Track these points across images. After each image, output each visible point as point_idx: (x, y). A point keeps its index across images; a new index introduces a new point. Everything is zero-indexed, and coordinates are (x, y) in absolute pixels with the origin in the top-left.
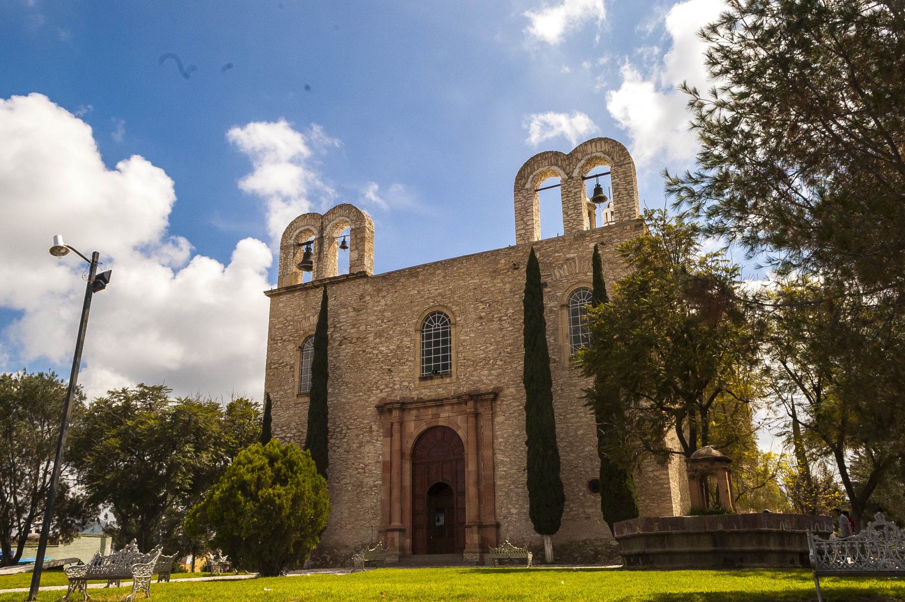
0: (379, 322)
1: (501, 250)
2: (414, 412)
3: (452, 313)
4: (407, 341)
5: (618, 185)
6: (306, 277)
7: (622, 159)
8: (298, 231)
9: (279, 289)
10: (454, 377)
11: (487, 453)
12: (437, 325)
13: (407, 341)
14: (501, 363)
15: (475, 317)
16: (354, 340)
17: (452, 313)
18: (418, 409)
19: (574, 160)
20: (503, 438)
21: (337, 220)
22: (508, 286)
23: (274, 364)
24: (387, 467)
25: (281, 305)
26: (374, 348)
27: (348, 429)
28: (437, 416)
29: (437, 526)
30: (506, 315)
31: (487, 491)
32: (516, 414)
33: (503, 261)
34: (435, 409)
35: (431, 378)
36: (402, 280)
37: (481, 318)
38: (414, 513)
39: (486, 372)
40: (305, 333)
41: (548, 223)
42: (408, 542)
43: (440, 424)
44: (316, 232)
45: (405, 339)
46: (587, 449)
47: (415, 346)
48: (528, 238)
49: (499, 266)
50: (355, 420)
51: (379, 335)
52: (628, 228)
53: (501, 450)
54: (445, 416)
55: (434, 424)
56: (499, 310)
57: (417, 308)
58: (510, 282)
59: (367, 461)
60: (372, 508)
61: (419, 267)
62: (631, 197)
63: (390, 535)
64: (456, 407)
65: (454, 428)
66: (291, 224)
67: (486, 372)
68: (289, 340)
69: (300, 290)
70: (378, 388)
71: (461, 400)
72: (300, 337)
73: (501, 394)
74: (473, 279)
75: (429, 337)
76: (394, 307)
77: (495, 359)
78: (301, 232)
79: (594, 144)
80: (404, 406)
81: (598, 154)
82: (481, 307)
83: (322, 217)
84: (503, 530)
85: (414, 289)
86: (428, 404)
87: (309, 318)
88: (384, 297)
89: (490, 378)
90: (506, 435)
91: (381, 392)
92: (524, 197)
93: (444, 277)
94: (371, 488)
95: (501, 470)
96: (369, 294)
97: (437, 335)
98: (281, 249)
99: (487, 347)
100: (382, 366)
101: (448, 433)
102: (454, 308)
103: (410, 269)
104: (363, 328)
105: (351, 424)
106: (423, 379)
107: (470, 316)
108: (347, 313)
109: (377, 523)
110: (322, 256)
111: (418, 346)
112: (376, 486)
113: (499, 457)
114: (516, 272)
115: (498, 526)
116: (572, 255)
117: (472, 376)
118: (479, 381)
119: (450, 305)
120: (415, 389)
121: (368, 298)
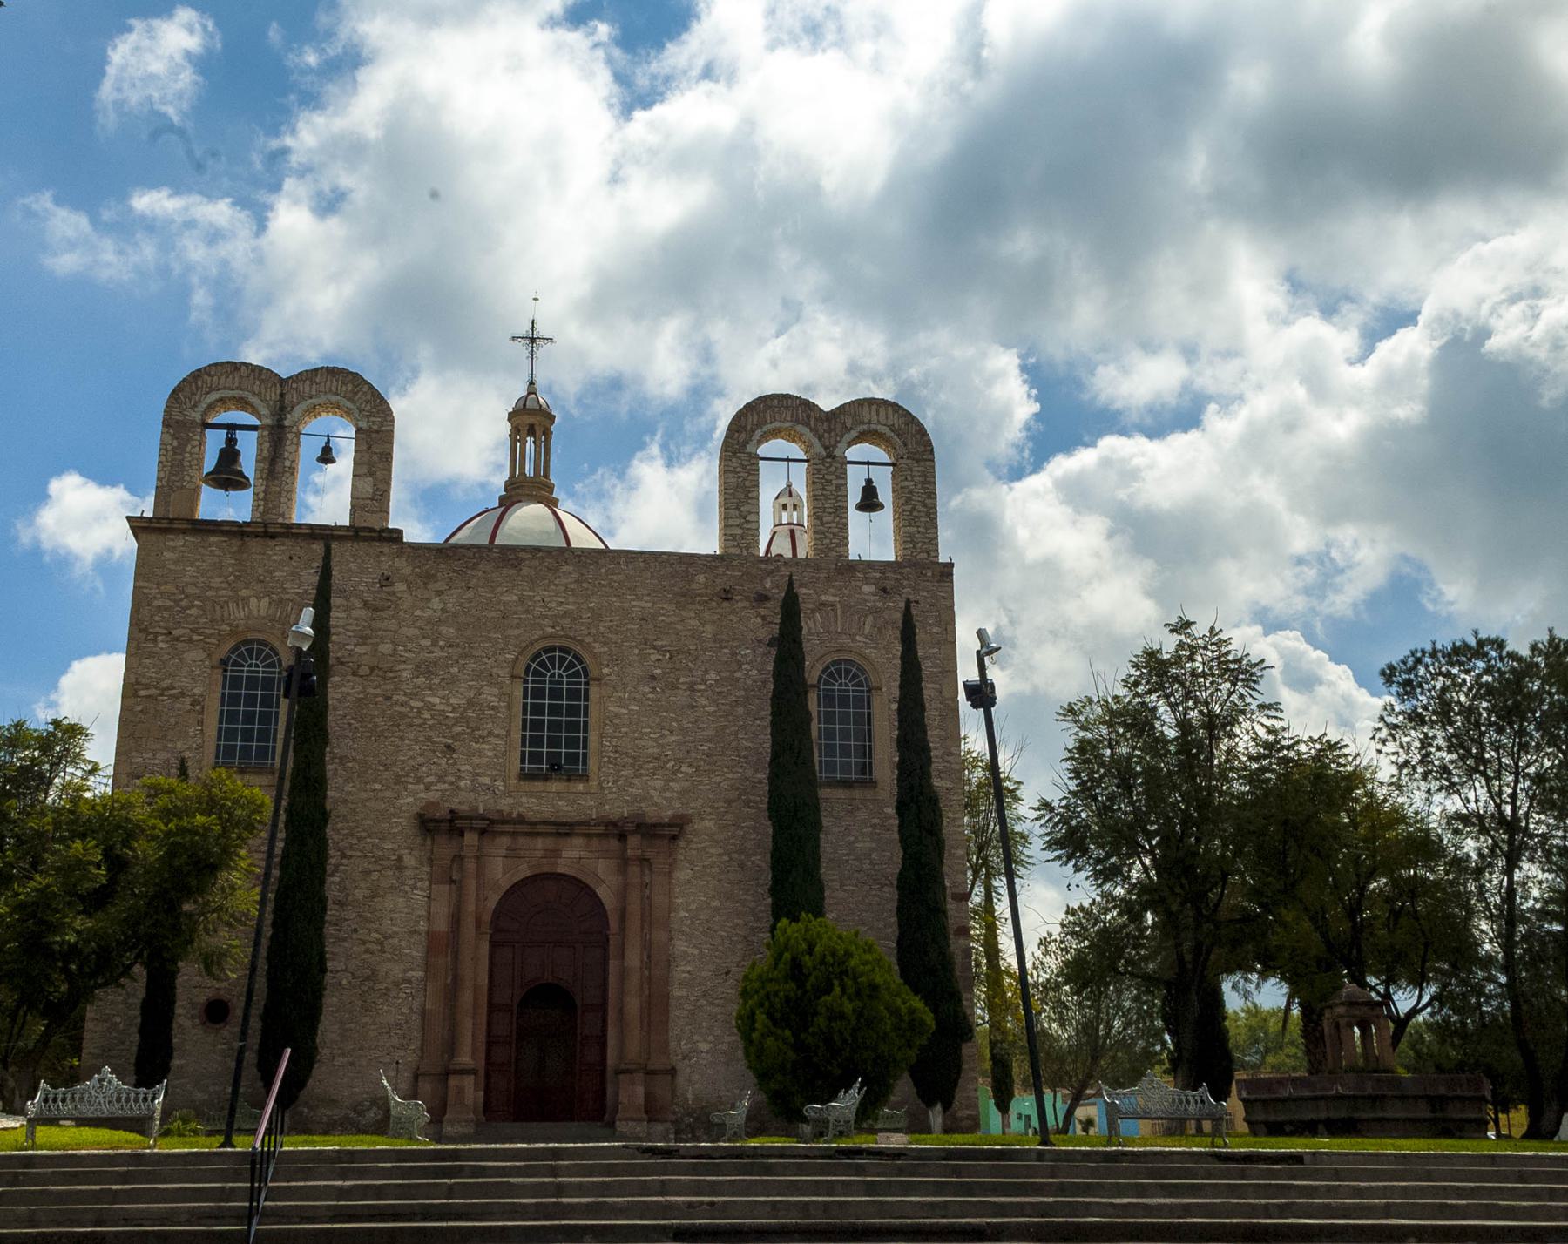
4: (490, 695)
5: (911, 492)
6: (235, 507)
8: (214, 396)
9: (155, 519)
11: (659, 936)
12: (556, 676)
13: (490, 695)
14: (690, 771)
15: (639, 672)
16: (365, 670)
17: (595, 656)
18: (514, 834)
19: (839, 427)
21: (322, 398)
22: (708, 627)
23: (147, 687)
24: (443, 945)
25: (168, 555)
26: (413, 696)
27: (343, 856)
28: (555, 853)
30: (704, 682)
31: (657, 1005)
34: (549, 842)
37: (653, 678)
39: (659, 784)
40: (233, 633)
41: (775, 525)
43: (560, 870)
44: (264, 411)
47: (509, 707)
48: (748, 547)
49: (694, 586)
50: (359, 839)
54: (572, 857)
57: (516, 632)
60: (399, 1026)
64: (595, 842)
66: (196, 376)
68: (190, 641)
70: (419, 780)
71: (617, 830)
73: (688, 828)
74: (638, 598)
75: (537, 693)
76: (463, 619)
78: (222, 400)
79: (874, 407)
80: (489, 826)
81: (883, 429)
82: (653, 658)
83: (282, 382)
85: (509, 591)
86: (541, 828)
87: (246, 600)
88: (439, 593)
89: (668, 795)
90: (693, 907)
91: (427, 789)
92: (742, 466)
94: (397, 984)
95: (681, 971)
96: (404, 580)
97: (556, 694)
98: (166, 423)
99: (663, 736)
101: (581, 889)
102: (598, 648)
105: (351, 847)
106: (525, 776)
108: (348, 609)
109: (410, 1057)
110: (279, 467)
113: (680, 945)
114: (726, 604)
116: (831, 599)
117: (631, 785)
118: (644, 799)
119: (588, 639)
120: (508, 793)
121: (401, 587)
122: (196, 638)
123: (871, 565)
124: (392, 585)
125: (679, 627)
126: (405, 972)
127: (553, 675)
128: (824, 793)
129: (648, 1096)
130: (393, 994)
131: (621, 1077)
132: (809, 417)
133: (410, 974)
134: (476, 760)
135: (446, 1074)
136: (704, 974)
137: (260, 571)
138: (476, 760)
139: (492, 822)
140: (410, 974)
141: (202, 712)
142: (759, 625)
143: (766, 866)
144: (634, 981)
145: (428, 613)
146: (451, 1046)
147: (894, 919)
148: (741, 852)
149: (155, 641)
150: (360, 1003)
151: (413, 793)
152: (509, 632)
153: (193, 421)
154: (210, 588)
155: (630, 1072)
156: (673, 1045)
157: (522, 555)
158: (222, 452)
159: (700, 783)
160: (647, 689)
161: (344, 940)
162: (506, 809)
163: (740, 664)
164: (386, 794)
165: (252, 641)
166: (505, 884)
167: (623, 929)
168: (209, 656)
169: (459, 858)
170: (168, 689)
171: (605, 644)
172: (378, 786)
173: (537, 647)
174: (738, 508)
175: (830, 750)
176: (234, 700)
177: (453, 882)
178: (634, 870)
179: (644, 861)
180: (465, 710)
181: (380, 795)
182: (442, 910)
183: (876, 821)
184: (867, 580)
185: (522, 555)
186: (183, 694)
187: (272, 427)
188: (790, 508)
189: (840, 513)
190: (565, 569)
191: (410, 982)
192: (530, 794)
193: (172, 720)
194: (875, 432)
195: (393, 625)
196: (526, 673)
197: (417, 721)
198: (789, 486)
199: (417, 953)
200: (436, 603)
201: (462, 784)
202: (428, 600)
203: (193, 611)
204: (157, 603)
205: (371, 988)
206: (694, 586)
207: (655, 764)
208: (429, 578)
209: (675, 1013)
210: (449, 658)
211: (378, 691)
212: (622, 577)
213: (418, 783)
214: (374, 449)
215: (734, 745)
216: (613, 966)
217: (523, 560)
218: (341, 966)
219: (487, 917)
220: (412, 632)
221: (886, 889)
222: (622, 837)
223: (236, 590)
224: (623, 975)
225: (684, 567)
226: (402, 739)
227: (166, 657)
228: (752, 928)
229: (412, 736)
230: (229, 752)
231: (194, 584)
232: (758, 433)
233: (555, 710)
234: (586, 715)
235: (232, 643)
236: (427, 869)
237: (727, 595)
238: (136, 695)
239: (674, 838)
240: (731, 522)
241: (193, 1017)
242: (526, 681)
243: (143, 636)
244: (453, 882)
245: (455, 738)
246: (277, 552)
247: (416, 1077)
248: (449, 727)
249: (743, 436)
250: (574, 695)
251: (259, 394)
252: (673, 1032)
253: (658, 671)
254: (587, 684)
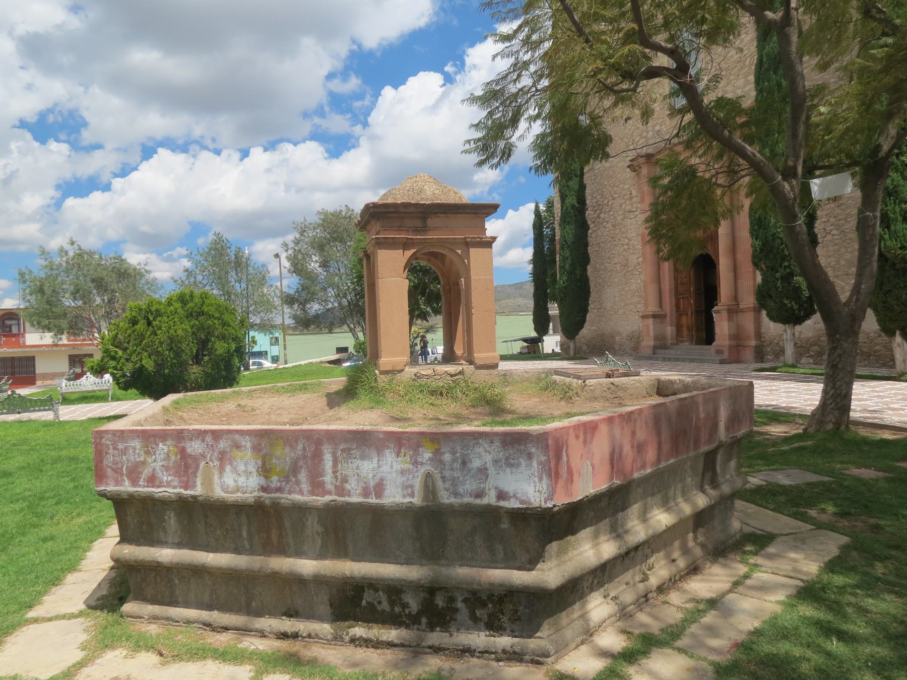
27: (614, 199)
38: (678, 295)
42: (669, 330)
105: (615, 193)
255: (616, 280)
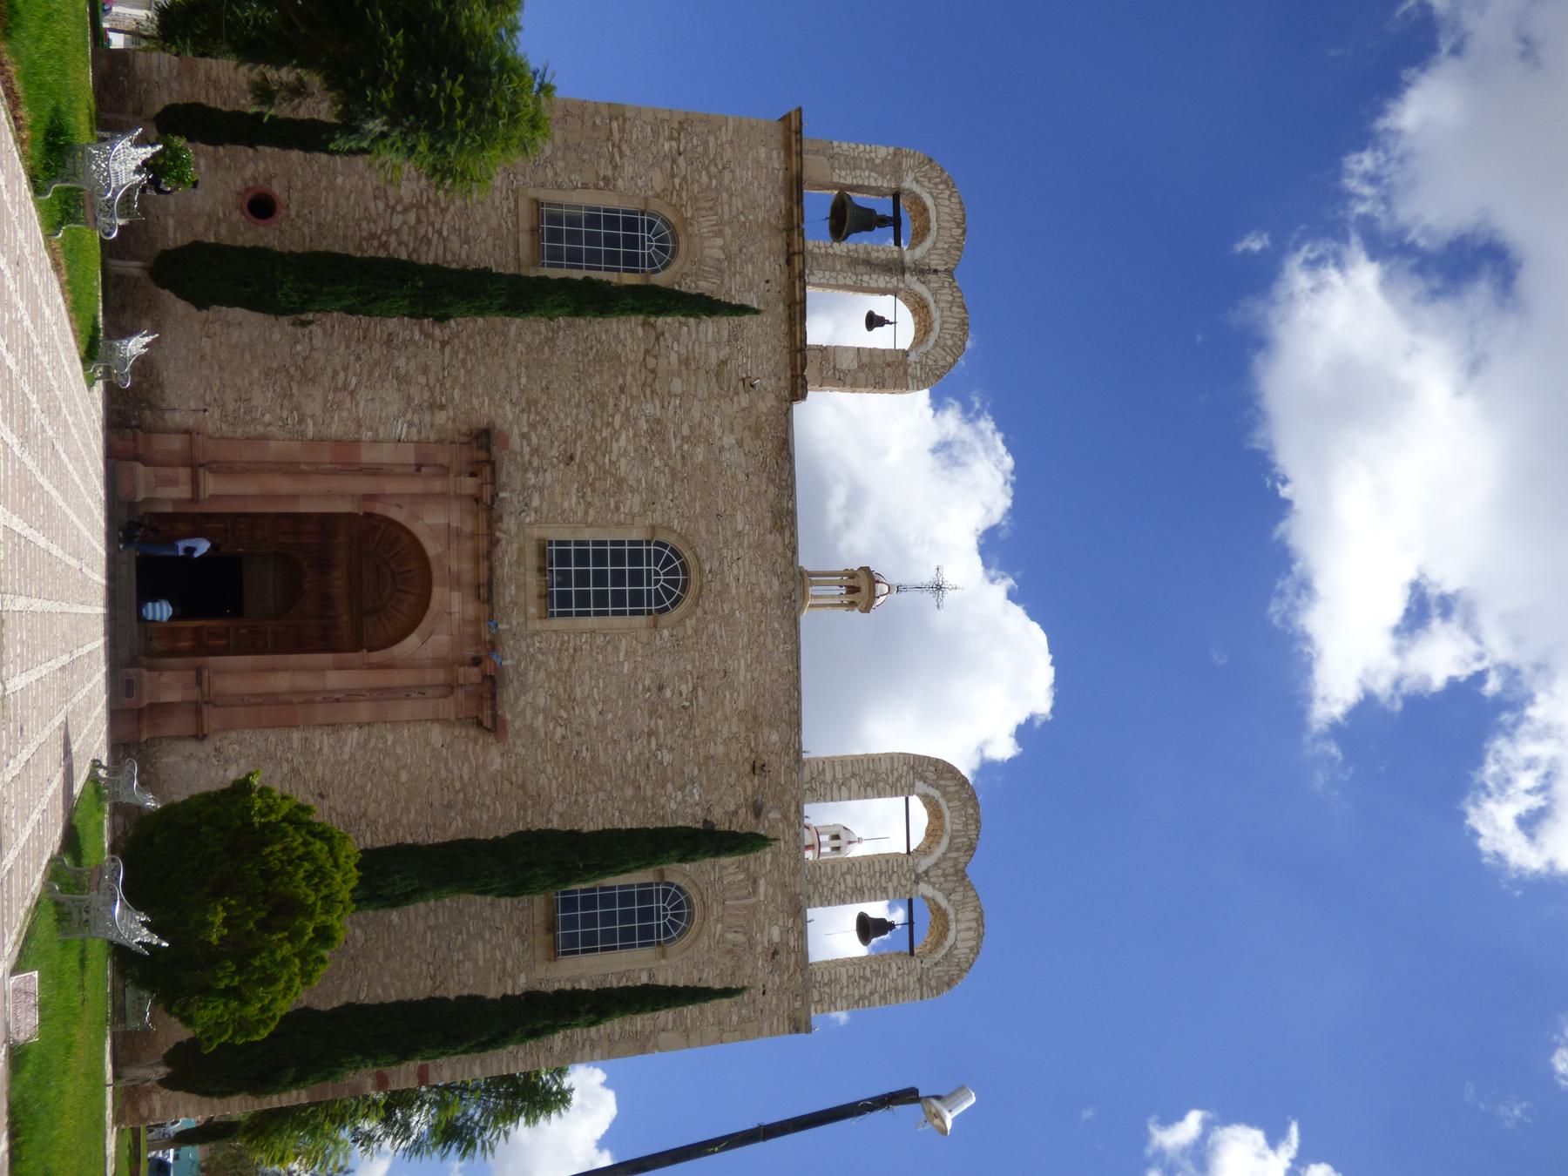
0: (685, 430)
1: (798, 734)
2: (468, 526)
3: (682, 620)
4: (632, 503)
5: (885, 975)
7: (933, 983)
8: (929, 202)
10: (538, 625)
11: (364, 710)
13: (632, 503)
15: (666, 672)
17: (682, 620)
19: (950, 885)
20: (394, 744)
22: (721, 749)
23: (622, 130)
24: (346, 458)
25: (763, 152)
26: (626, 414)
27: (444, 344)
28: (455, 582)
29: (203, 578)
31: (278, 711)
32: (443, 774)
33: (775, 737)
34: (467, 577)
35: (542, 570)
36: (772, 490)
37: (661, 688)
39: (541, 701)
40: (684, 220)
43: (438, 593)
45: (637, 499)
46: (358, 932)
47: (620, 524)
48: (812, 790)
49: (766, 730)
50: (464, 361)
51: (657, 430)
52: (797, 1005)
53: (367, 741)
54: (451, 605)
55: (436, 574)
56: (672, 731)
57: (703, 530)
58: (727, 755)
59: (364, 395)
61: (793, 535)
62: (857, 1002)
63: (184, 473)
65: (424, 626)
67: (541, 701)
68: (673, 176)
69: (790, 212)
70: (533, 426)
72: (678, 209)
73: (491, 739)
74: (748, 667)
75: (636, 557)
76: (714, 469)
77: (567, 723)
78: (925, 209)
79: (974, 924)
80: (487, 508)
81: (951, 935)
82: (683, 687)
84: (191, 747)
87: (720, 234)
88: (740, 443)
89: (529, 712)
90: (399, 750)
91: (524, 436)
93: (762, 598)
94: (297, 408)
95: (323, 741)
97: (636, 578)
99: (595, 703)
100: (582, 431)
102: (690, 623)
103: (792, 514)
104: (677, 386)
105: (454, 353)
107: (668, 660)
108: (717, 343)
109: (213, 422)
110: (861, 269)
111: (618, 535)
112: (301, 421)
113: (354, 737)
114: (748, 767)
115: (200, 737)
116: (762, 890)
117: (538, 669)
118: (523, 685)
119: (699, 612)
120: (521, 525)
121: (744, 400)
122: (677, 181)
123: (802, 934)
124: (747, 391)
125: (719, 715)
126: (312, 417)
127: (657, 573)
128: (539, 900)
129: (168, 708)
130: (286, 402)
131: (193, 673)
132: (958, 850)
133: (310, 422)
134: (558, 488)
135: (194, 466)
136: (319, 768)
137: (752, 249)
138: (558, 488)
139: (490, 508)
140: (310, 422)
141: (597, 187)
142: (725, 807)
143: (449, 836)
144: (307, 681)
145: (719, 433)
146: (224, 469)
147: (392, 996)
148: (468, 804)
149: (671, 138)
150: (275, 365)
151: (518, 419)
152: (702, 523)
153: (901, 179)
154: (731, 196)
155: (199, 683)
156: (233, 735)
157: (787, 533)
158: (871, 211)
159: (545, 750)
160: (647, 683)
161: (348, 347)
162: (504, 526)
163: (682, 788)
164: (515, 392)
165: (676, 241)
166: (418, 529)
167: (371, 666)
168: (658, 196)
169: (444, 471)
170: (620, 151)
171: (696, 631)
172: (523, 380)
173: (687, 554)
174: (853, 775)
175: (589, 902)
176: (612, 222)
177: (419, 467)
178: (440, 676)
179: (450, 687)
180: (614, 476)
181: (514, 383)
182: (384, 455)
183: (509, 965)
184: (785, 931)
185: (787, 533)
186: (615, 167)
187: (902, 262)
188: (836, 843)
189: (859, 894)
190: (776, 582)
191: (301, 421)
192: (521, 551)
193: (586, 157)
194: (946, 928)
195: (702, 392)
196: (658, 543)
197: (598, 423)
198: (860, 840)
199: (335, 429)
200: (729, 440)
201: (530, 475)
202: (732, 431)
203: (705, 178)
204: (711, 139)
205: (292, 378)
206: (766, 730)
207: (564, 697)
208: (756, 431)
209: (273, 736)
210: (670, 457)
211: (629, 378)
212: (770, 647)
213: (529, 425)
214: (887, 370)
215: (590, 787)
216: (327, 658)
217: (782, 534)
218: (317, 343)
219: (379, 509)
220: (696, 413)
221: (429, 983)
222: (476, 661)
223: (730, 223)
224: (320, 670)
225: (786, 717)
226: (578, 405)
227: (654, 149)
228: (375, 822)
229: (581, 417)
230: (555, 219)
231: (733, 180)
232: (936, 794)
233: (618, 578)
234: (615, 613)
235: (673, 219)
236: (433, 437)
237: (757, 768)
238: (611, 118)
239: (479, 724)
240: (838, 768)
241: (255, 179)
242: (648, 543)
243: (676, 125)
244: (419, 467)
245: (582, 466)
246: (772, 267)
247: (187, 432)
248: (593, 459)
249: (931, 776)
250: (637, 598)
251: (934, 248)
252: (248, 735)
253: (668, 694)
254: (650, 613)
255: (277, 336)
